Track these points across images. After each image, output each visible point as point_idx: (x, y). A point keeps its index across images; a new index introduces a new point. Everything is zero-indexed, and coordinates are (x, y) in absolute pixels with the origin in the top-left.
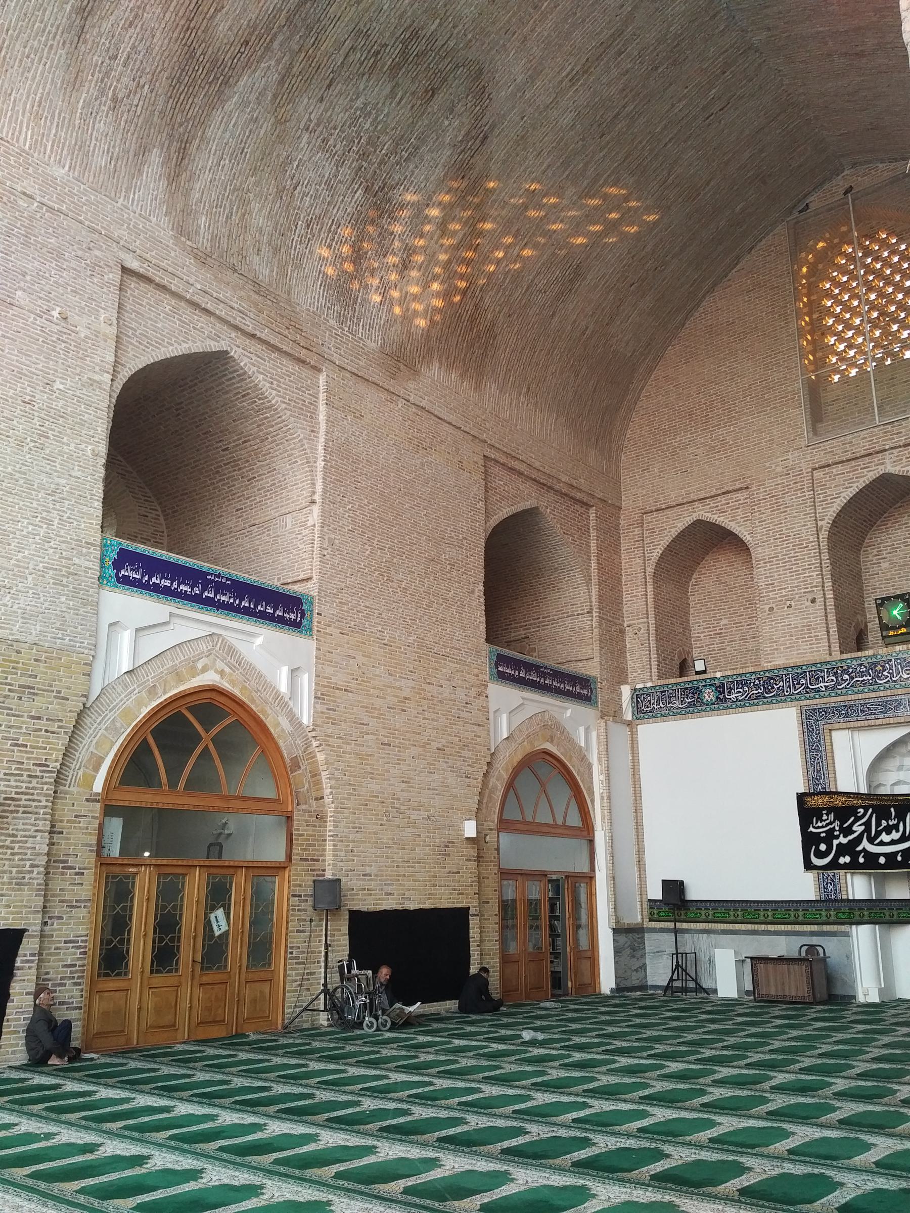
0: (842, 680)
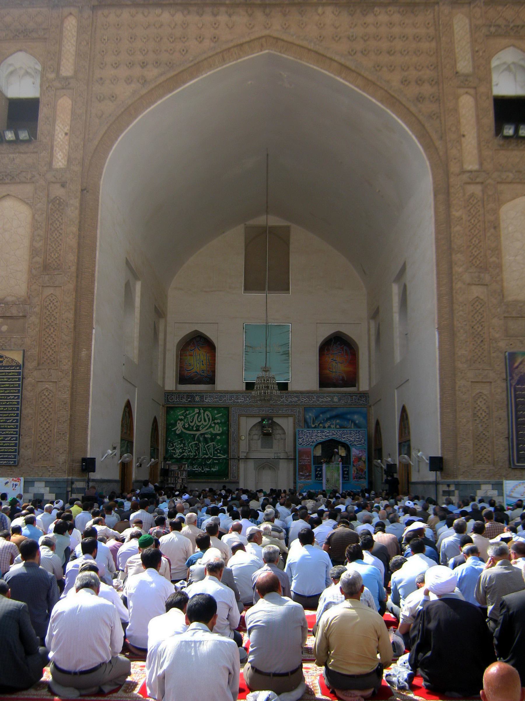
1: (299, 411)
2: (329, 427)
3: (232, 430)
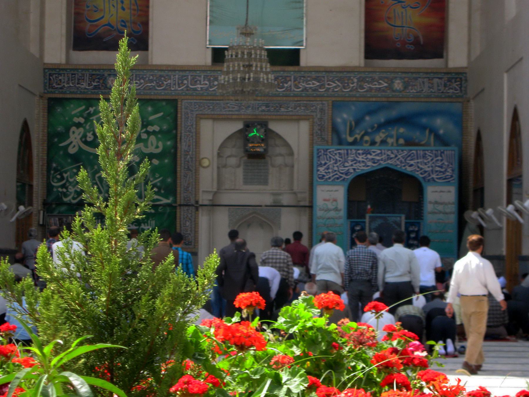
0: (213, 85)
1: (322, 110)
2: (384, 142)
3: (183, 146)
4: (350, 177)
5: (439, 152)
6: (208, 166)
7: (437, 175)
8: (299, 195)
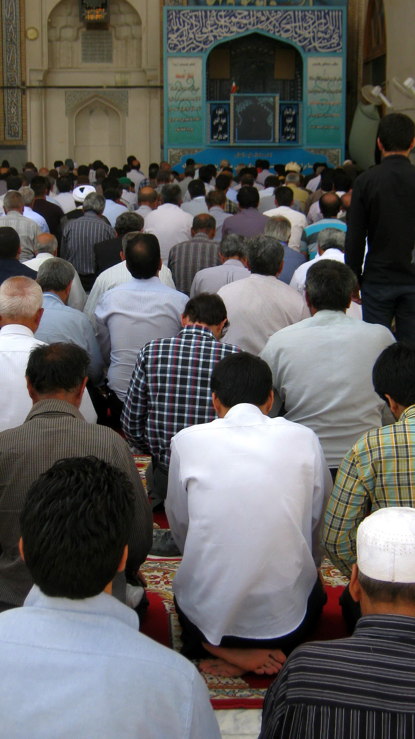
4: (210, 47)
5: (323, 13)
6: (35, 39)
7: (321, 43)
8: (149, 74)
